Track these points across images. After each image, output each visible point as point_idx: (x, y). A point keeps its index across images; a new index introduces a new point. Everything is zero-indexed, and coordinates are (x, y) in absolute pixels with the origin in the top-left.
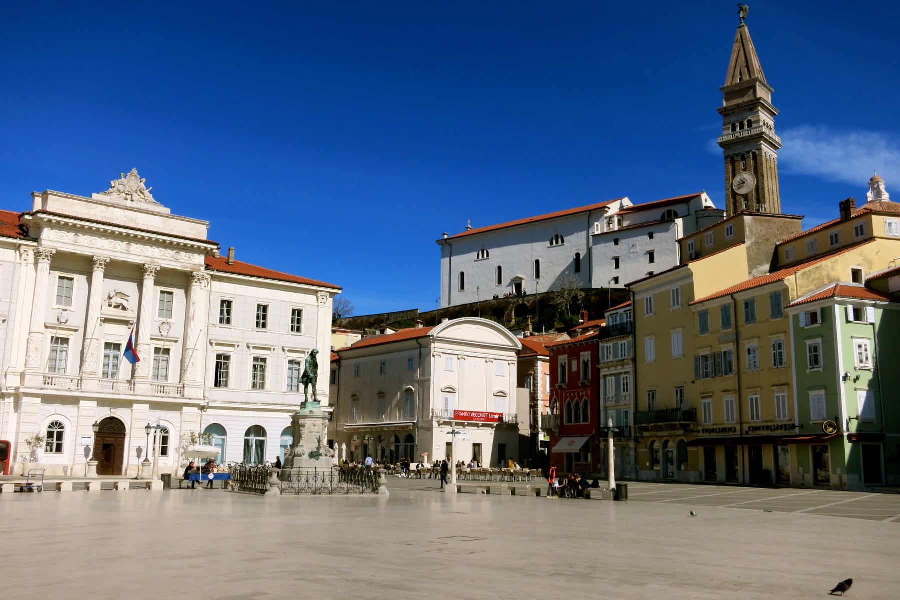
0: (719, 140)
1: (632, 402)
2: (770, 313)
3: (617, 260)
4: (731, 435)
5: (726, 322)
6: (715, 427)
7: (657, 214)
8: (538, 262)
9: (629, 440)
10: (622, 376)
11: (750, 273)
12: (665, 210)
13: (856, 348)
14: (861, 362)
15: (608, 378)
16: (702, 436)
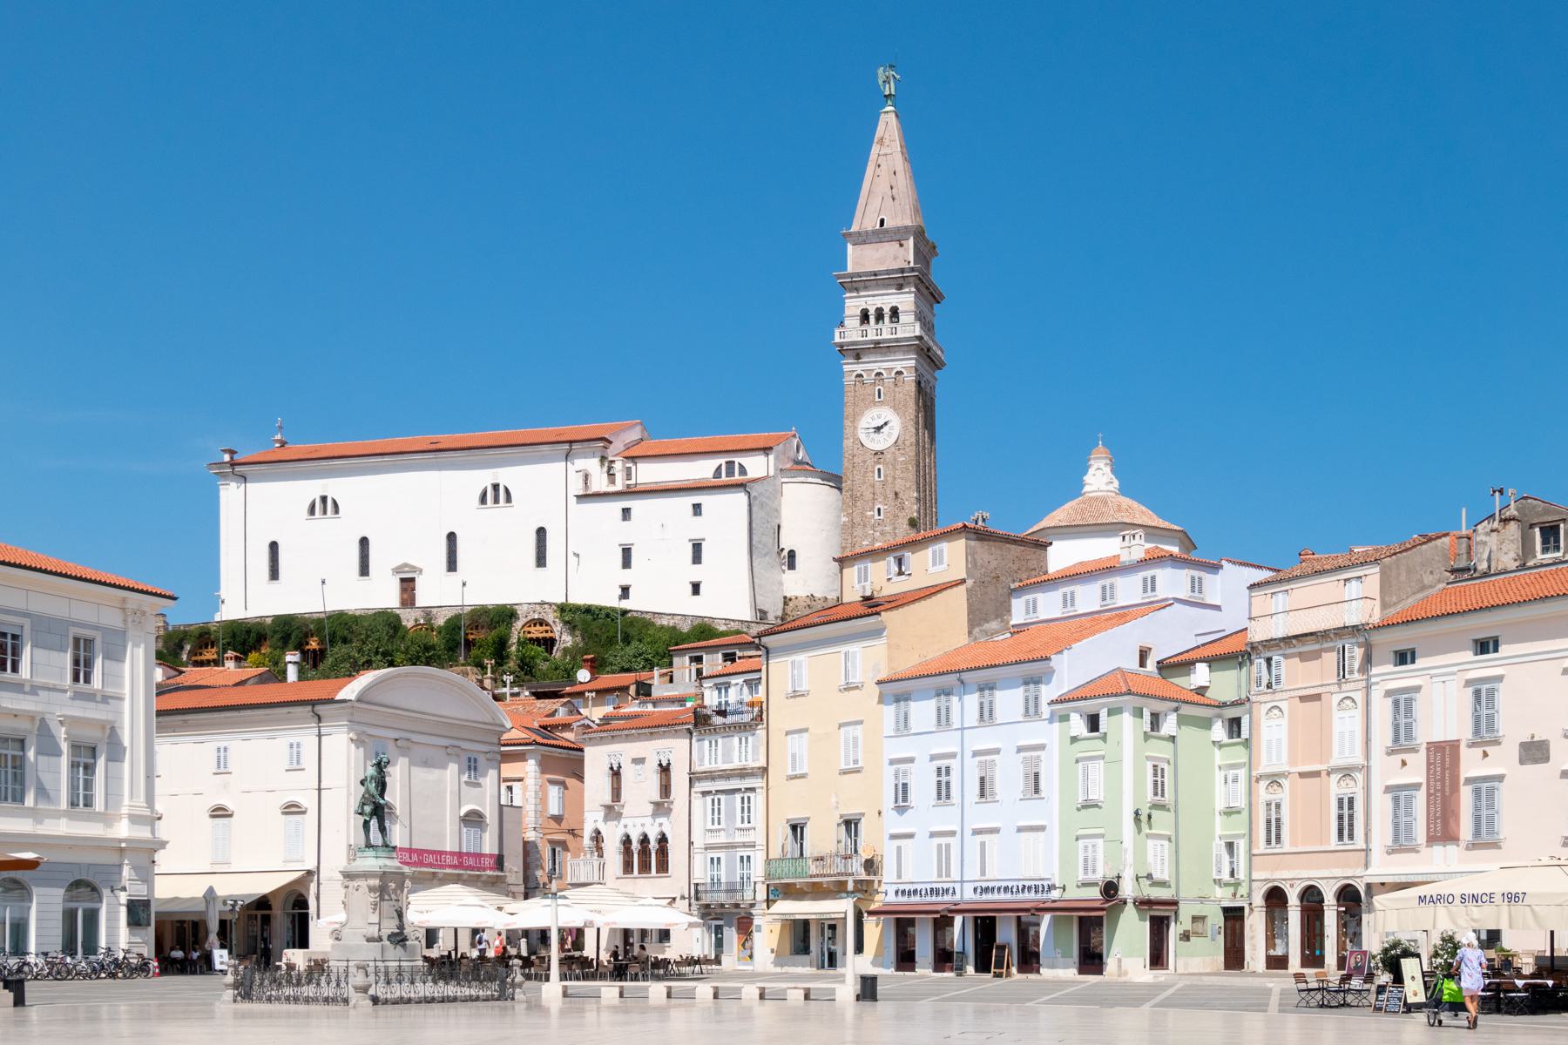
0: (837, 340)
1: (760, 839)
2: (1022, 710)
3: (627, 553)
4: (947, 898)
5: (943, 718)
6: (919, 887)
7: (703, 469)
8: (452, 537)
9: (752, 906)
10: (738, 797)
11: (970, 633)
12: (722, 461)
13: (1150, 771)
14: (1156, 794)
15: (709, 798)
16: (891, 898)
